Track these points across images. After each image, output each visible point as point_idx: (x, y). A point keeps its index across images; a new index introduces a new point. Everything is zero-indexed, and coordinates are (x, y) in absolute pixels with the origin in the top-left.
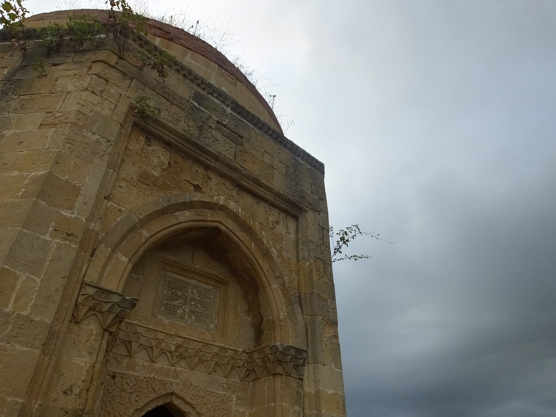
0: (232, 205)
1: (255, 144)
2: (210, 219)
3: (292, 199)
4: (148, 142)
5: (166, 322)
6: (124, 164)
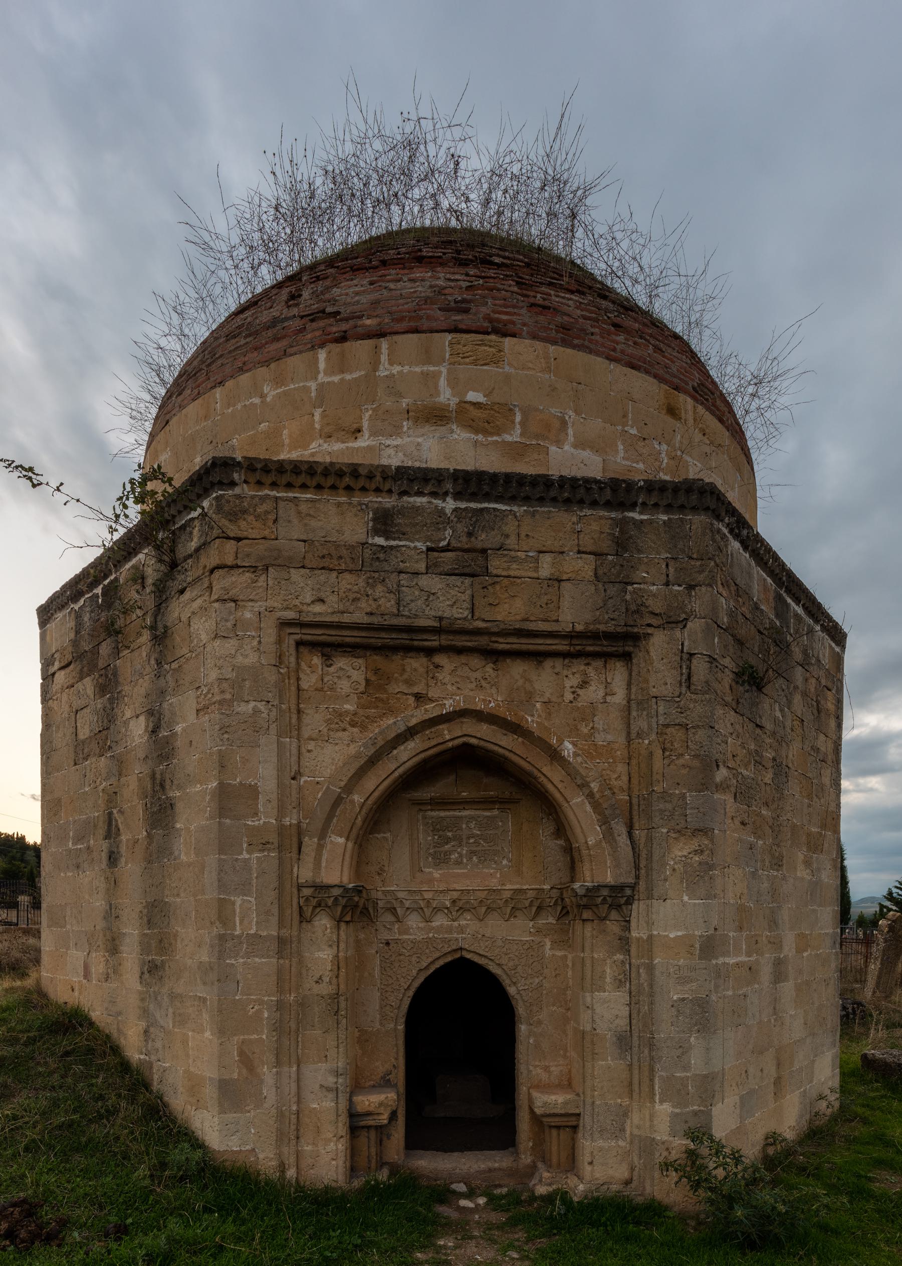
1: (516, 547)
2: (448, 737)
3: (610, 628)
4: (327, 659)
6: (305, 716)
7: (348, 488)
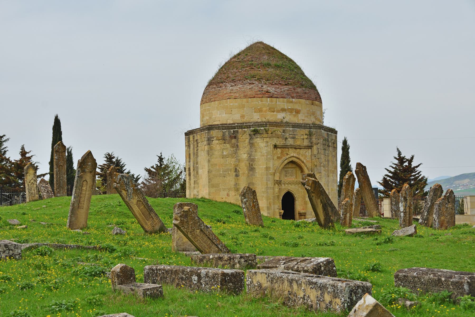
0: (295, 155)
5: (286, 178)
7: (280, 127)
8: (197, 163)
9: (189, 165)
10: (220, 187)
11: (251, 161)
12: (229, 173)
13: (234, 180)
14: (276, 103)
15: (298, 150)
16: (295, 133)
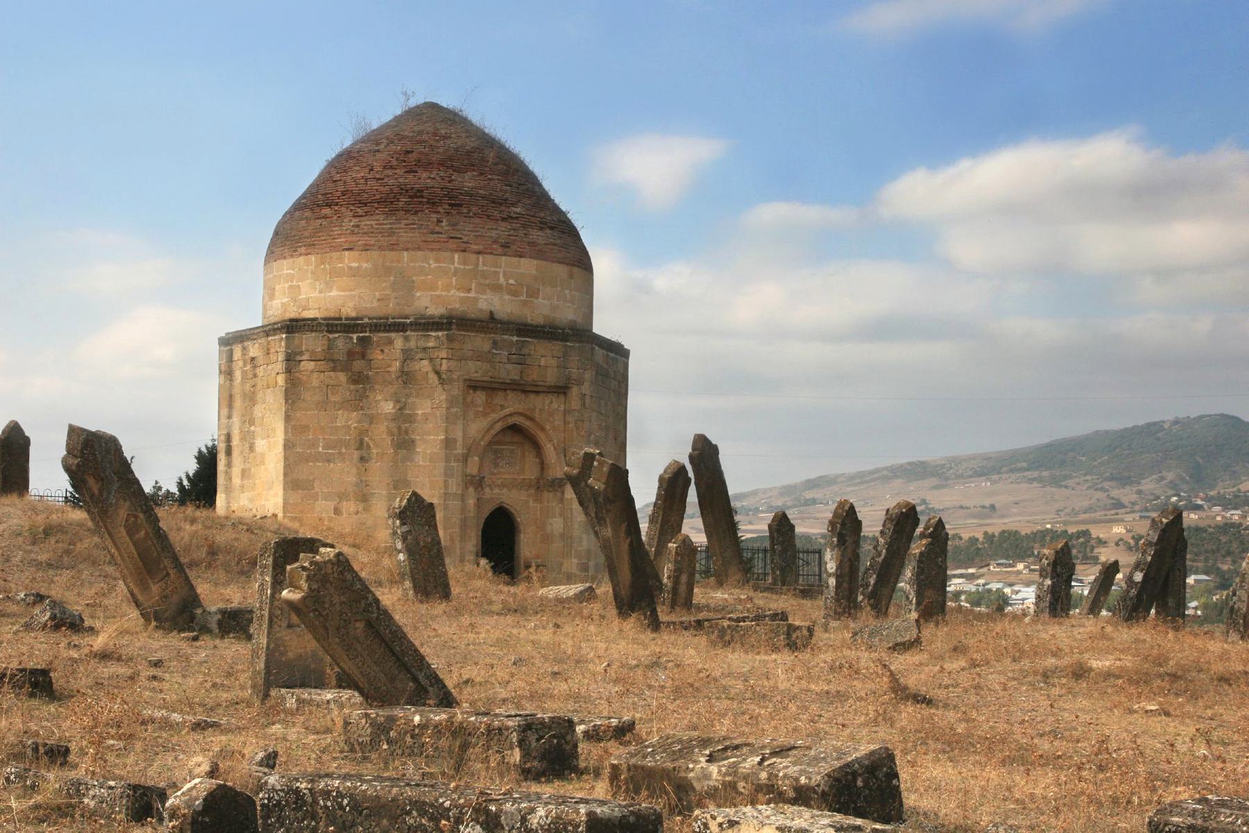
3: (561, 384)
8: (252, 422)
9: (229, 427)
10: (316, 490)
11: (405, 421)
12: (343, 450)
13: (354, 470)
14: (477, 265)
15: (532, 396)
16: (525, 351)
